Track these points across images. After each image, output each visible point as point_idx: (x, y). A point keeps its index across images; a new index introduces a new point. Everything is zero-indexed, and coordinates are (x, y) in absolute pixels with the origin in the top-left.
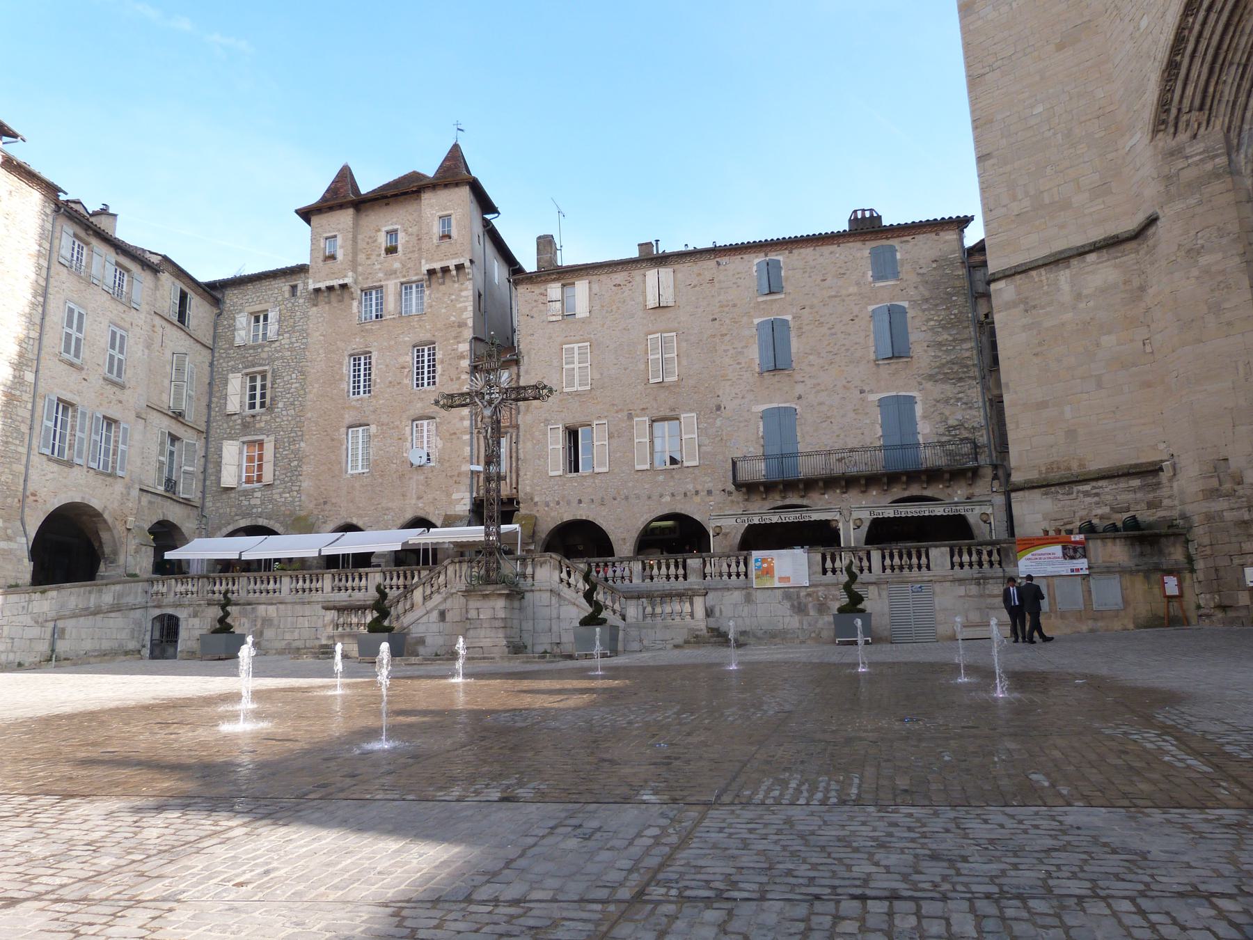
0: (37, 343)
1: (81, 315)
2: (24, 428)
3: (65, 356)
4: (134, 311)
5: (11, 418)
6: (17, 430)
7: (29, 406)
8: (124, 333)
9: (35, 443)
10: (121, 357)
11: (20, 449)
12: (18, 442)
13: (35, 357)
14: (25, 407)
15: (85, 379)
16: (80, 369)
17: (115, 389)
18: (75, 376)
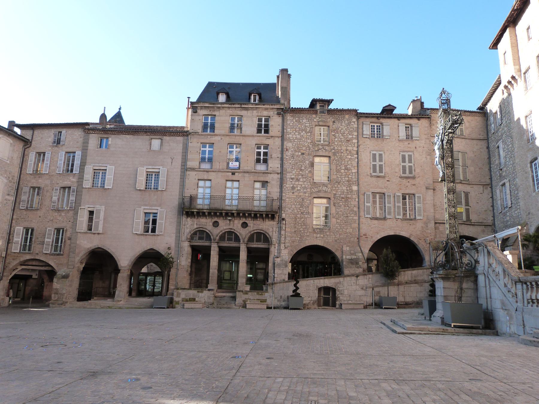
0: (357, 174)
1: (380, 155)
2: (356, 209)
3: (374, 174)
4: (417, 141)
5: (348, 206)
6: (352, 210)
7: (357, 200)
8: (410, 153)
9: (362, 214)
10: (410, 164)
11: (355, 218)
12: (353, 215)
13: (357, 180)
14: (355, 201)
15: (388, 181)
16: (384, 177)
17: (409, 180)
18: (381, 180)
